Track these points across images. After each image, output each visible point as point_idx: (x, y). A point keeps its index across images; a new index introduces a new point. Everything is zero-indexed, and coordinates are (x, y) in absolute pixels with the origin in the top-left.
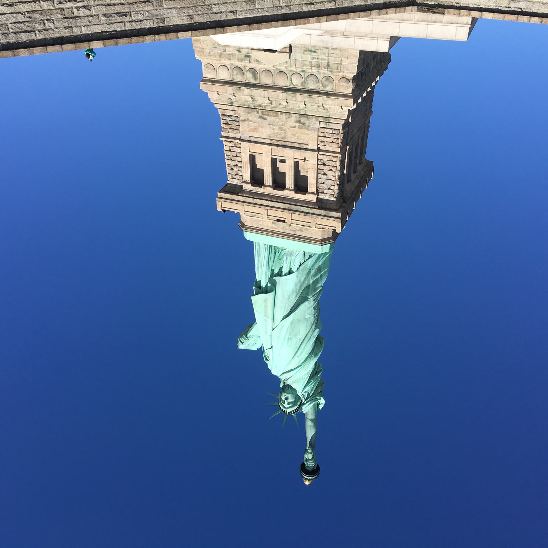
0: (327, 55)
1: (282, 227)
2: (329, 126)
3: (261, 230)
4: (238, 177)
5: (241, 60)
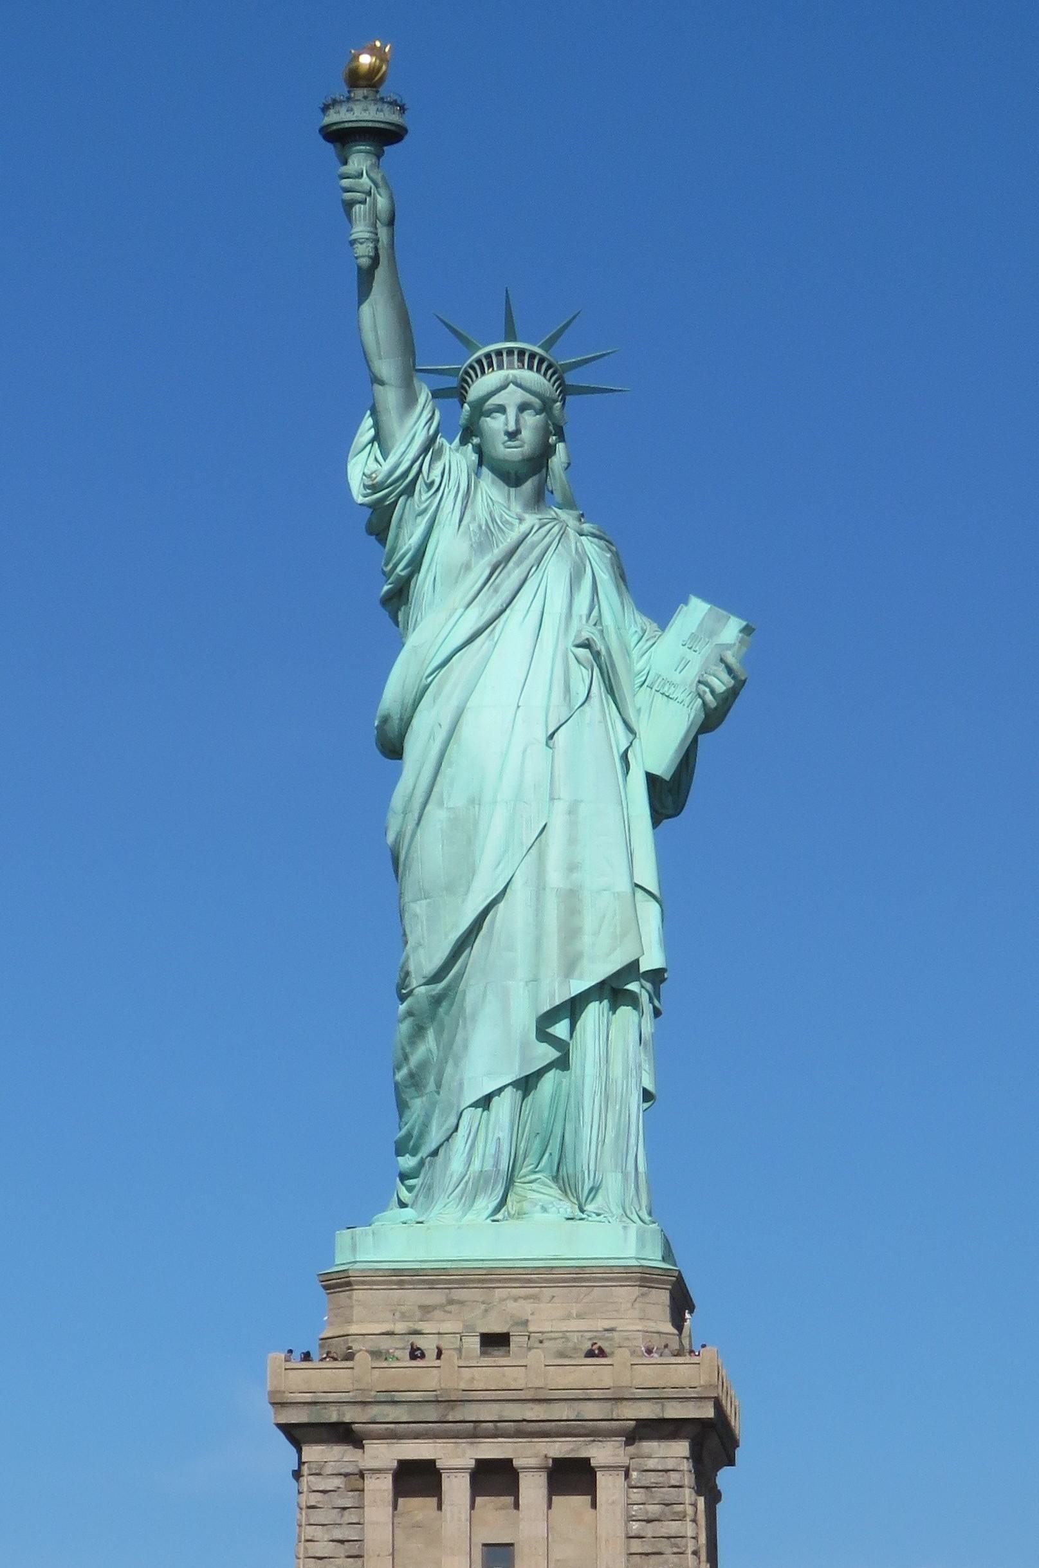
3: (574, 1280)
4: (645, 1480)
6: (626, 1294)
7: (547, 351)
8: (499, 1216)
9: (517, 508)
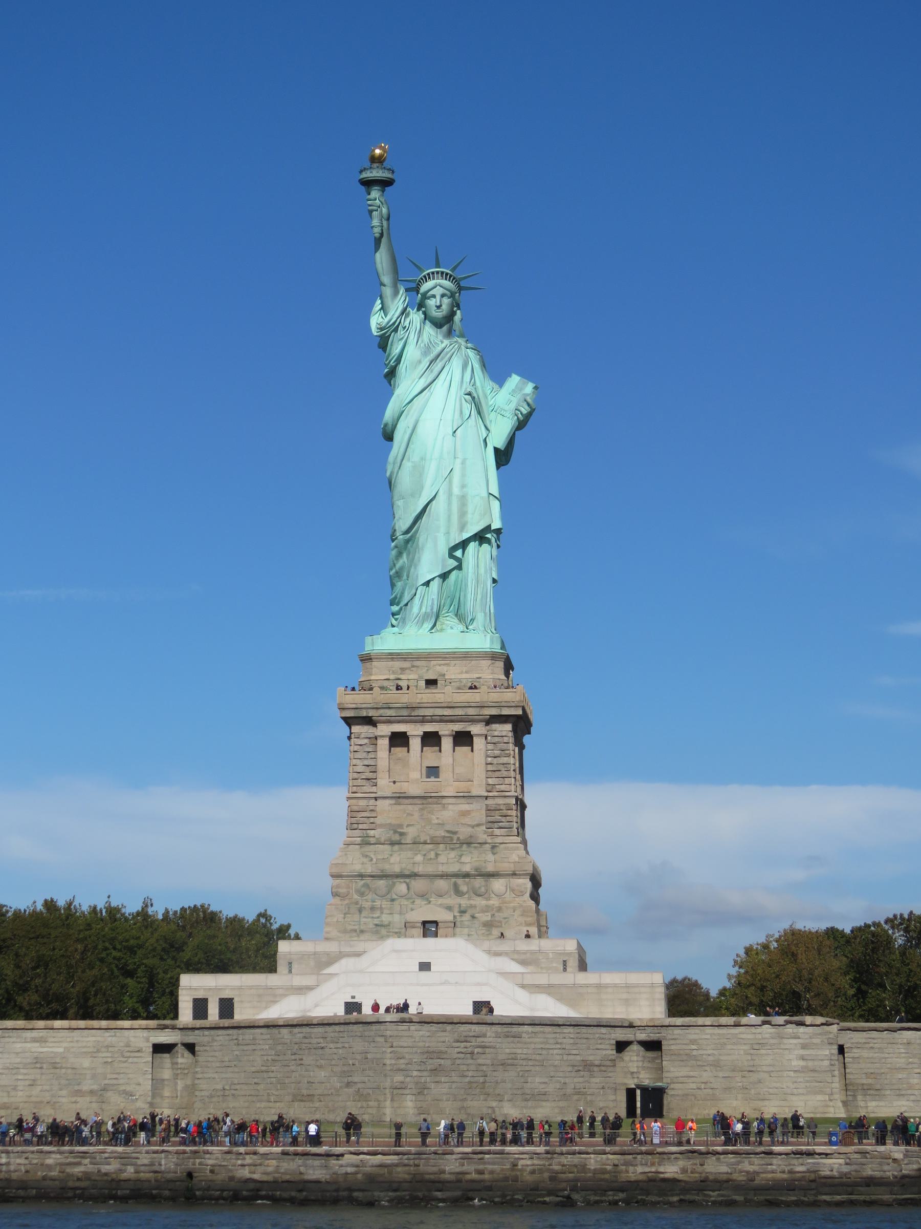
0: (362, 923)
1: (430, 671)
2: (363, 833)
5: (472, 906)
6: (486, 663)
7: (453, 272)
8: (433, 631)
9: (440, 337)
